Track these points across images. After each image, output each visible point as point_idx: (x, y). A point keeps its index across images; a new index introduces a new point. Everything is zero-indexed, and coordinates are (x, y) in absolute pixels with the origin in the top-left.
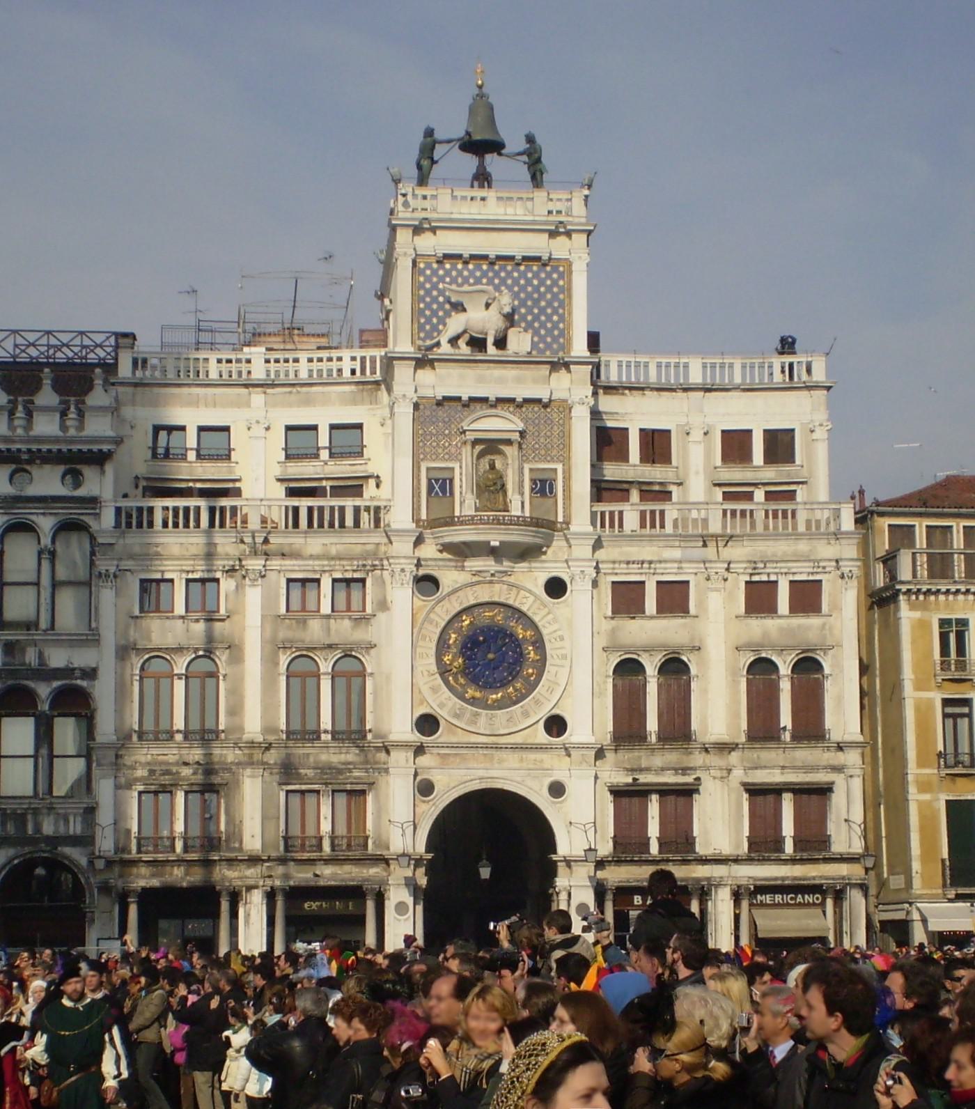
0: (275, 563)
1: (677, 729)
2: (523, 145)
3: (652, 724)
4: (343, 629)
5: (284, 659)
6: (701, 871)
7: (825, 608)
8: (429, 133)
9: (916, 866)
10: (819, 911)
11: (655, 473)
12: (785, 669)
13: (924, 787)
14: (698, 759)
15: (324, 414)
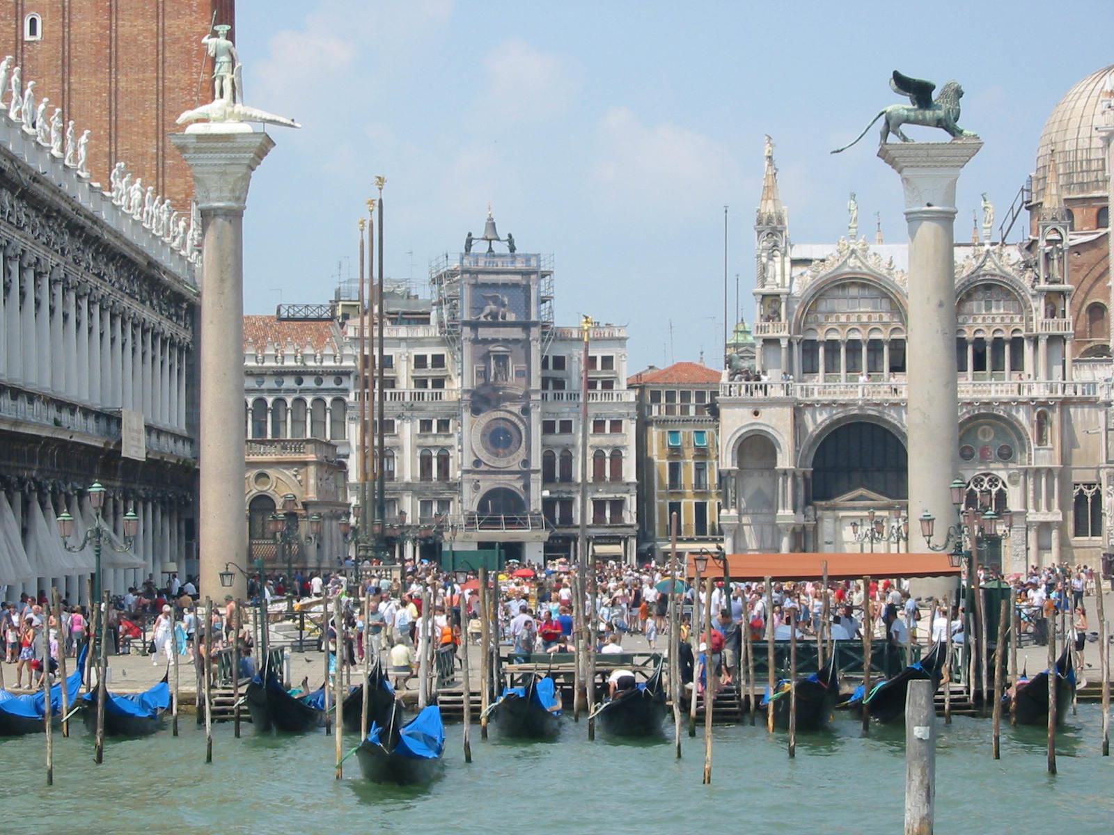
0: (416, 414)
1: (567, 477)
2: (507, 238)
3: (557, 474)
4: (442, 441)
5: (419, 452)
6: (574, 531)
7: (623, 431)
8: (470, 235)
9: (657, 528)
10: (618, 547)
11: (558, 374)
12: (608, 454)
13: (661, 497)
14: (574, 489)
15: (429, 352)
